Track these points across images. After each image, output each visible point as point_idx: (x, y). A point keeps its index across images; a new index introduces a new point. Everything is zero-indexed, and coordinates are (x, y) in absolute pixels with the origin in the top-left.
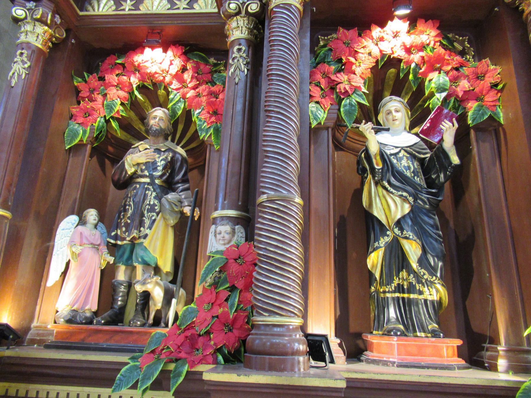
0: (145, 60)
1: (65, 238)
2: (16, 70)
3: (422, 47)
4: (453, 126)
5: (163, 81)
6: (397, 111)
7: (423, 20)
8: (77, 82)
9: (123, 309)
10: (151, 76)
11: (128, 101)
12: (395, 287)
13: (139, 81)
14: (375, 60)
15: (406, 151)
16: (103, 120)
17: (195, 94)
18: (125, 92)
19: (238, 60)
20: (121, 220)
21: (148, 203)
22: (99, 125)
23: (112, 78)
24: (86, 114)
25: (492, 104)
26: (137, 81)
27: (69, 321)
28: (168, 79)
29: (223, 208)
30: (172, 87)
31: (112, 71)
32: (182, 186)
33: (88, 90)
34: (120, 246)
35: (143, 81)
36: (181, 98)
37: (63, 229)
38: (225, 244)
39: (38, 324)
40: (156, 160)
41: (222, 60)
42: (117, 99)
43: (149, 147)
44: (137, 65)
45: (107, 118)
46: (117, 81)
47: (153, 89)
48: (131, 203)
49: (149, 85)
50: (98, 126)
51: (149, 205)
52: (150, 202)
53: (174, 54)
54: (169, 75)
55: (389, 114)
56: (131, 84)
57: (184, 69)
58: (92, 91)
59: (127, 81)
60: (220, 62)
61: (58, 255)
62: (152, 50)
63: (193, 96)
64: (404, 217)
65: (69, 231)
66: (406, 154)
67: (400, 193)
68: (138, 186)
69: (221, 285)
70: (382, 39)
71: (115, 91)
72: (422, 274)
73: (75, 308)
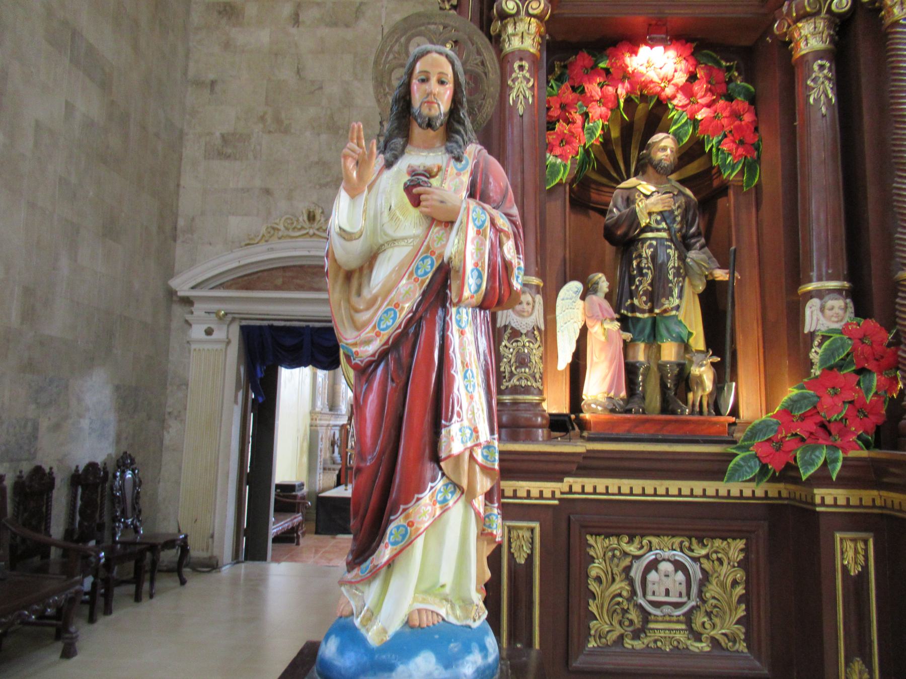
1: (567, 311)
5: (659, 94)
10: (645, 85)
19: (823, 83)
20: (637, 287)
23: (593, 89)
24: (562, 141)
26: (624, 93)
28: (669, 91)
29: (820, 279)
30: (675, 102)
33: (558, 106)
34: (638, 319)
35: (631, 93)
37: (563, 299)
38: (837, 322)
48: (651, 266)
49: (637, 98)
51: (674, 267)
54: (672, 86)
56: (617, 97)
57: (692, 77)
58: (564, 107)
62: (652, 48)
63: (711, 118)
65: (571, 301)
68: (654, 243)
69: (846, 368)
73: (612, 394)
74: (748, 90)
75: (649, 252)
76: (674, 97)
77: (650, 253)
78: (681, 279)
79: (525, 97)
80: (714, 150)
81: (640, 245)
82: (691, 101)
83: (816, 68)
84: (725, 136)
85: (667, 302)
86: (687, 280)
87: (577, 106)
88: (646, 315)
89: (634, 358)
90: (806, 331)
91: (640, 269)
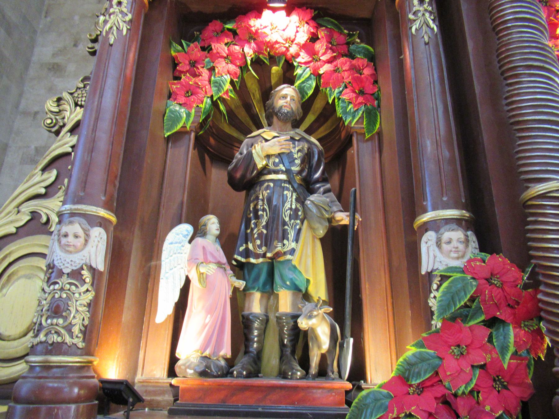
0: (264, 25)
1: (174, 256)
2: (115, 24)
5: (284, 54)
8: (174, 51)
9: (260, 352)
10: (271, 45)
11: (237, 78)
13: (254, 52)
16: (209, 101)
17: (332, 69)
18: (236, 66)
19: (423, 15)
20: (252, 230)
21: (290, 206)
22: (205, 106)
23: (221, 47)
24: (188, 92)
26: (251, 52)
27: (203, 374)
28: (293, 50)
29: (434, 209)
30: (298, 60)
31: (219, 41)
32: (323, 186)
33: (187, 62)
34: (253, 265)
35: (259, 53)
36: (311, 74)
37: (171, 243)
38: (458, 258)
39: (144, 378)
41: (356, 31)
42: (226, 75)
44: (254, 31)
45: (215, 99)
46: (227, 51)
47: (268, 64)
48: (266, 207)
49: (266, 58)
50: (205, 109)
51: (291, 209)
52: (291, 205)
53: (300, 19)
54: (295, 45)
56: (244, 56)
57: (314, 38)
58: (194, 64)
59: (239, 52)
60: (353, 32)
61: (167, 278)
63: (331, 71)
65: (180, 245)
68: (272, 185)
69: (472, 318)
71: (224, 64)
73: (207, 353)
74: (367, 50)
75: (266, 193)
76: (298, 55)
77: (266, 194)
78: (298, 221)
80: (336, 101)
81: (258, 188)
82: (314, 59)
84: (346, 87)
85: (280, 245)
86: (306, 222)
87: (205, 62)
88: (261, 260)
89: (249, 308)
90: (423, 273)
91: (256, 211)
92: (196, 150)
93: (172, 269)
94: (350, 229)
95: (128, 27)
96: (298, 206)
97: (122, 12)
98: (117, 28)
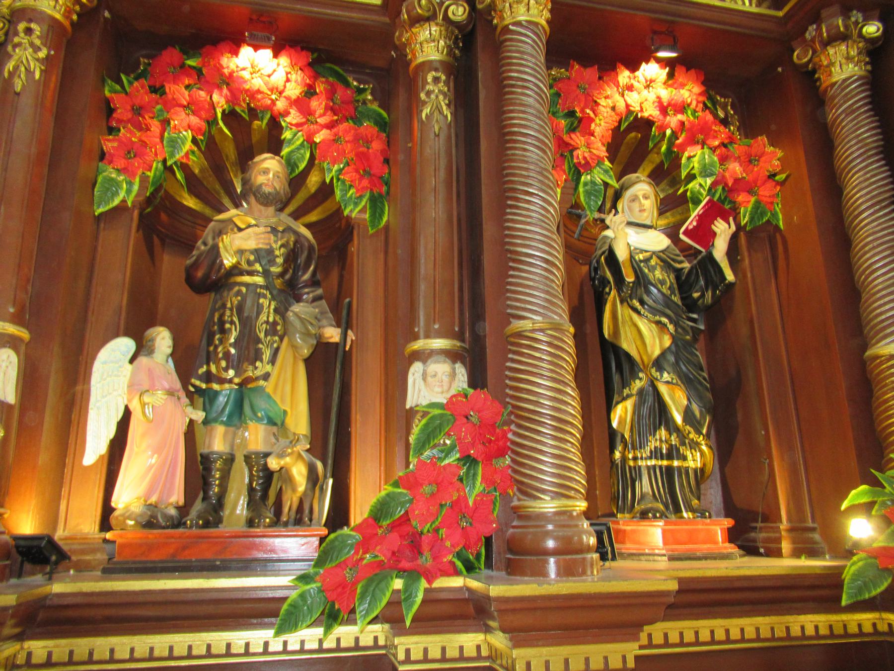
0: (241, 66)
1: (109, 379)
2: (22, 62)
3: (681, 108)
4: (730, 227)
6: (646, 197)
7: (684, 69)
8: (110, 91)
9: (221, 498)
10: (253, 94)
11: (203, 135)
12: (651, 452)
13: (227, 102)
14: (618, 119)
15: (659, 257)
16: (160, 165)
17: (332, 138)
18: (201, 118)
19: (437, 97)
20: (216, 347)
21: (265, 319)
22: (155, 174)
23: (179, 91)
24: (129, 152)
25: (769, 200)
26: (223, 102)
28: (281, 105)
30: (288, 119)
31: (176, 80)
32: (312, 292)
33: (129, 108)
35: (234, 104)
36: (304, 140)
39: (67, 533)
40: (271, 247)
41: (368, 83)
42: (186, 131)
43: (253, 222)
44: (227, 74)
45: (169, 163)
46: (188, 98)
47: (247, 118)
48: (236, 319)
49: (243, 111)
50: (154, 177)
51: (267, 322)
52: (268, 318)
53: (291, 62)
54: (284, 99)
55: (633, 200)
56: (213, 106)
57: (310, 92)
58: (139, 110)
59: (206, 100)
60: (364, 85)
61: (98, 408)
62: (256, 50)
63: (329, 140)
64: (663, 354)
65: (117, 365)
66: (659, 261)
67: (657, 318)
68: (244, 290)
70: (630, 88)
71: (183, 115)
72: (687, 432)
73: (153, 500)
74: (380, 115)
75: (236, 301)
76: (287, 113)
77: (236, 302)
78: (277, 338)
79: (27, 70)
80: (335, 181)
81: (225, 294)
82: (308, 120)
83: (430, 79)
84: (348, 164)
85: (251, 368)
86: (286, 339)
87: (155, 110)
89: (210, 446)
90: (408, 407)
91: (222, 323)
92: (141, 232)
93: (106, 396)
94: (341, 349)
95: (43, 68)
96: (278, 318)
97: (32, 45)
98: (26, 68)
